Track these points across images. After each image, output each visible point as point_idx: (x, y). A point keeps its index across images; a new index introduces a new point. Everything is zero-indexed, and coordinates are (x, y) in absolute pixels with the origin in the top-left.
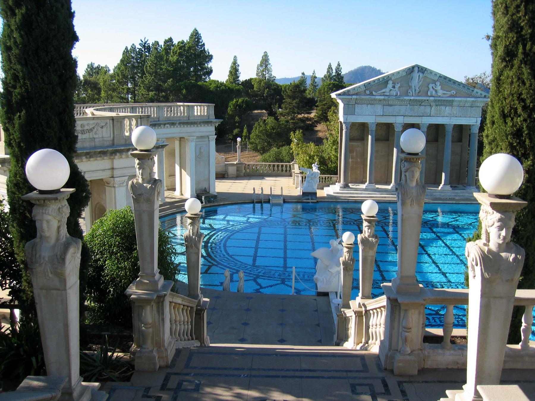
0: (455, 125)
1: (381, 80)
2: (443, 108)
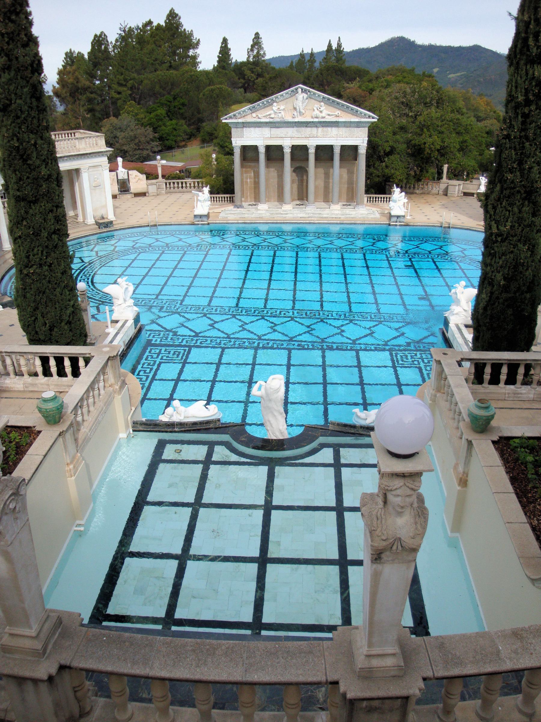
0: (342, 147)
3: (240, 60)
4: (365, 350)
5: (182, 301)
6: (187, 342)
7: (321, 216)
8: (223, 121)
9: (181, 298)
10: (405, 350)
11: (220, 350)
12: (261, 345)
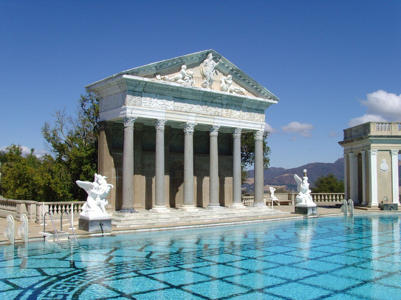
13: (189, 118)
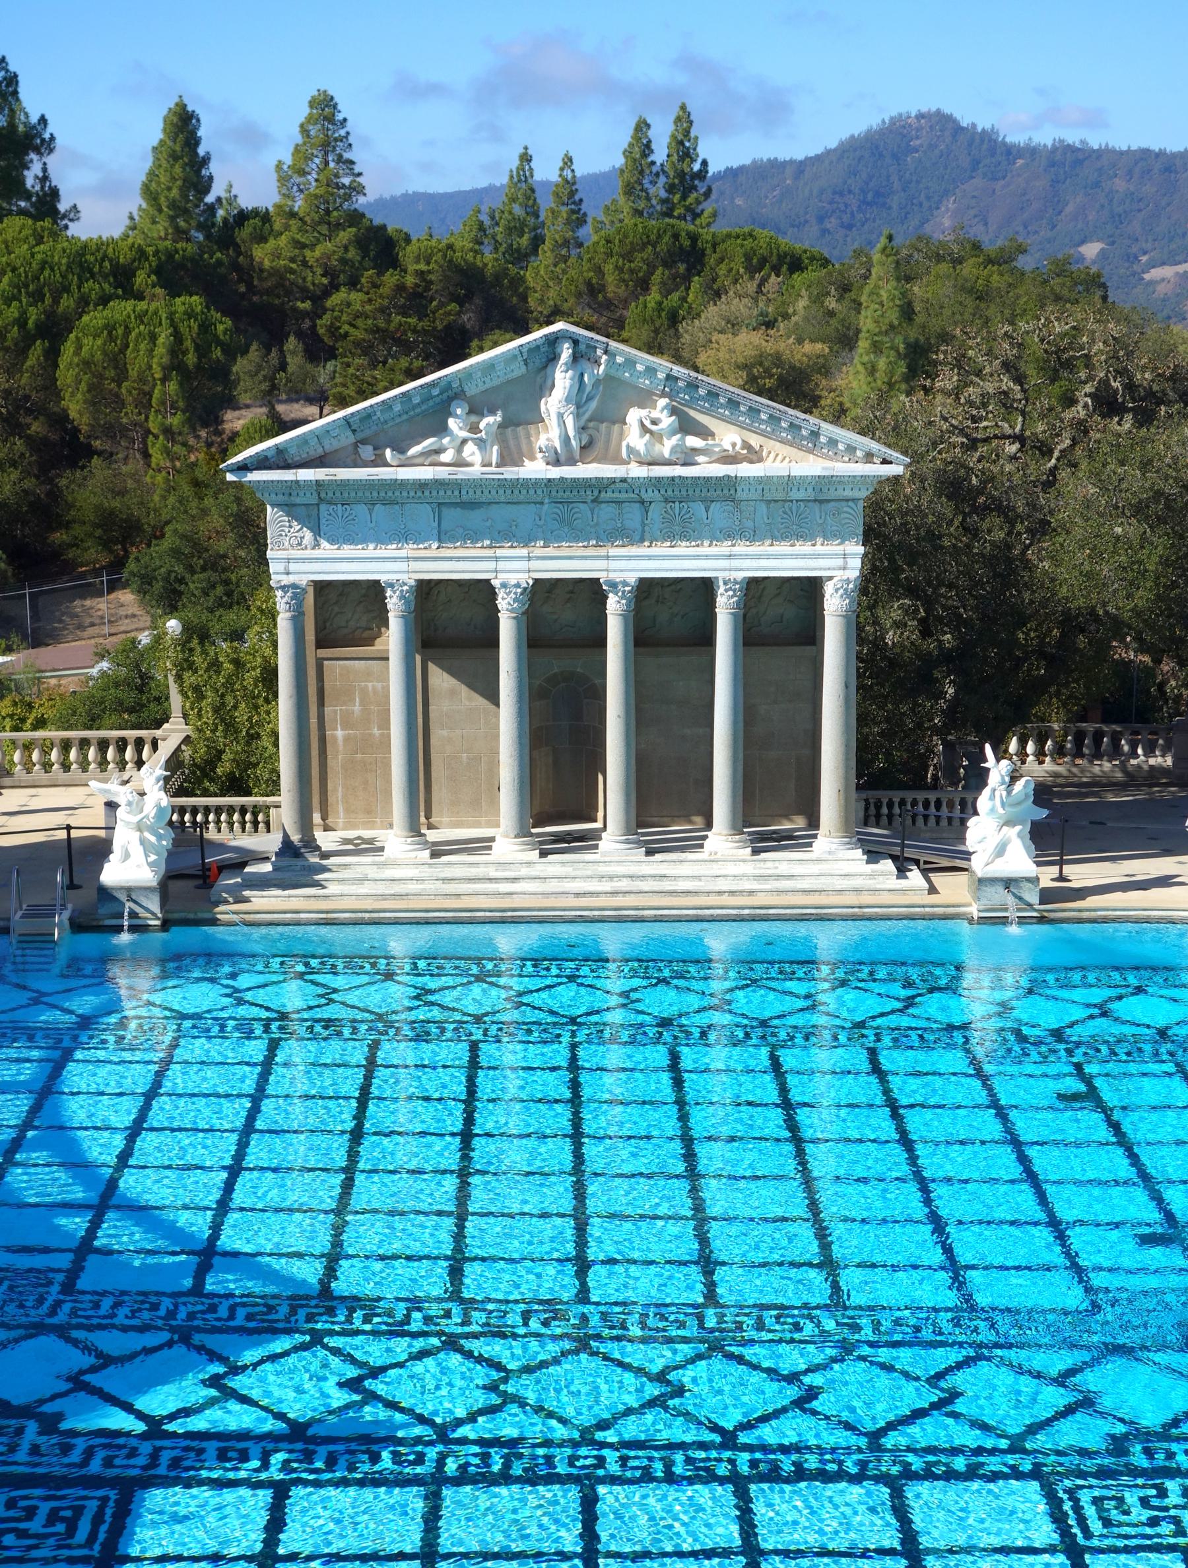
1: (416, 400)
2: (699, 508)
3: (247, 202)
4: (929, 1475)
5: (74, 1272)
6: (108, 1463)
7: (667, 885)
8: (230, 477)
9: (64, 1261)
10: (1103, 1473)
11: (265, 1496)
12: (451, 1466)
13: (502, 565)
